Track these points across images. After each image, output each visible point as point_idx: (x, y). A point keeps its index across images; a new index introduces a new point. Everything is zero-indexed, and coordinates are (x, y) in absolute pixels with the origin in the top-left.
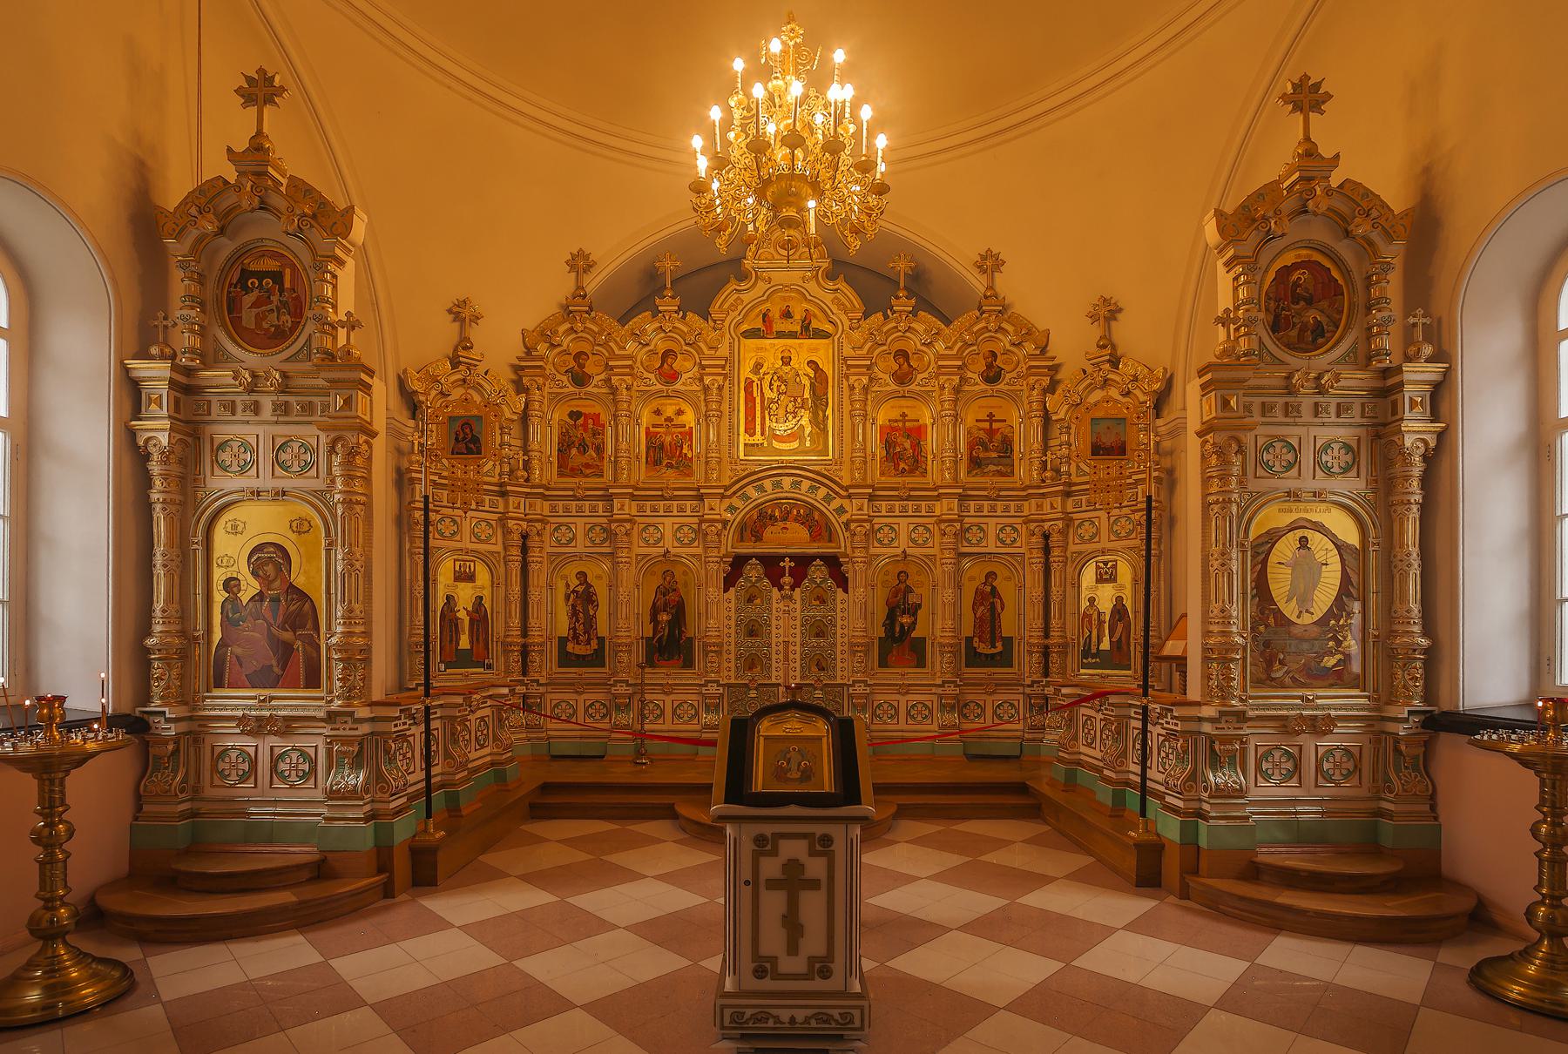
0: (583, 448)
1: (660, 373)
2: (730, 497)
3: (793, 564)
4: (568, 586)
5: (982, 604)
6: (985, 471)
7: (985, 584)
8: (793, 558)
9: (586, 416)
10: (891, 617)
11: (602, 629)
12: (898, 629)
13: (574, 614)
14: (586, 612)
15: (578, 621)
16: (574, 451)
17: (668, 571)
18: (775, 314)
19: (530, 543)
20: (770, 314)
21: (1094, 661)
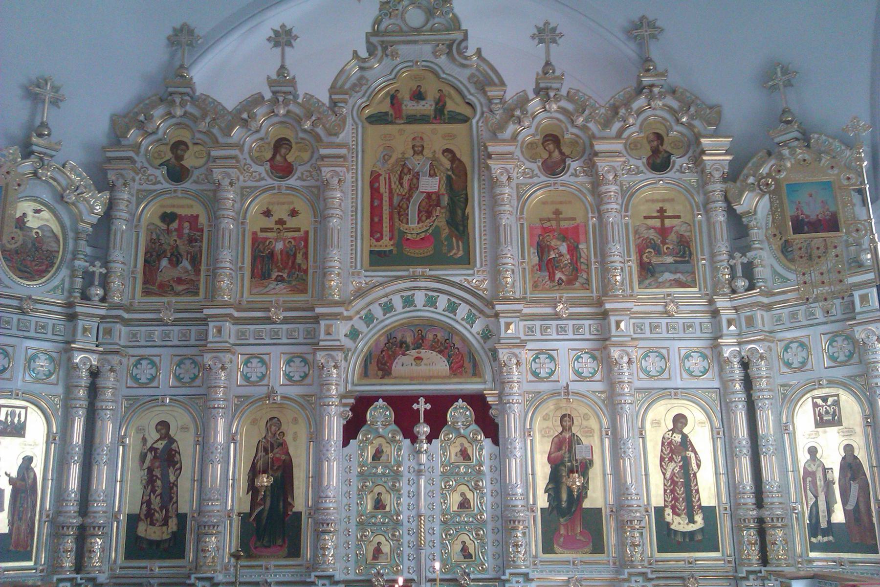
0: (175, 260)
1: (271, 166)
2: (350, 318)
3: (429, 406)
4: (144, 440)
5: (671, 459)
6: (660, 280)
7: (673, 430)
8: (429, 399)
9: (181, 218)
10: (555, 479)
11: (185, 502)
12: (564, 496)
13: (151, 480)
14: (165, 476)
15: (153, 491)
16: (164, 262)
17: (271, 419)
18: (405, 95)
19: (101, 382)
20: (399, 96)
21: (826, 539)
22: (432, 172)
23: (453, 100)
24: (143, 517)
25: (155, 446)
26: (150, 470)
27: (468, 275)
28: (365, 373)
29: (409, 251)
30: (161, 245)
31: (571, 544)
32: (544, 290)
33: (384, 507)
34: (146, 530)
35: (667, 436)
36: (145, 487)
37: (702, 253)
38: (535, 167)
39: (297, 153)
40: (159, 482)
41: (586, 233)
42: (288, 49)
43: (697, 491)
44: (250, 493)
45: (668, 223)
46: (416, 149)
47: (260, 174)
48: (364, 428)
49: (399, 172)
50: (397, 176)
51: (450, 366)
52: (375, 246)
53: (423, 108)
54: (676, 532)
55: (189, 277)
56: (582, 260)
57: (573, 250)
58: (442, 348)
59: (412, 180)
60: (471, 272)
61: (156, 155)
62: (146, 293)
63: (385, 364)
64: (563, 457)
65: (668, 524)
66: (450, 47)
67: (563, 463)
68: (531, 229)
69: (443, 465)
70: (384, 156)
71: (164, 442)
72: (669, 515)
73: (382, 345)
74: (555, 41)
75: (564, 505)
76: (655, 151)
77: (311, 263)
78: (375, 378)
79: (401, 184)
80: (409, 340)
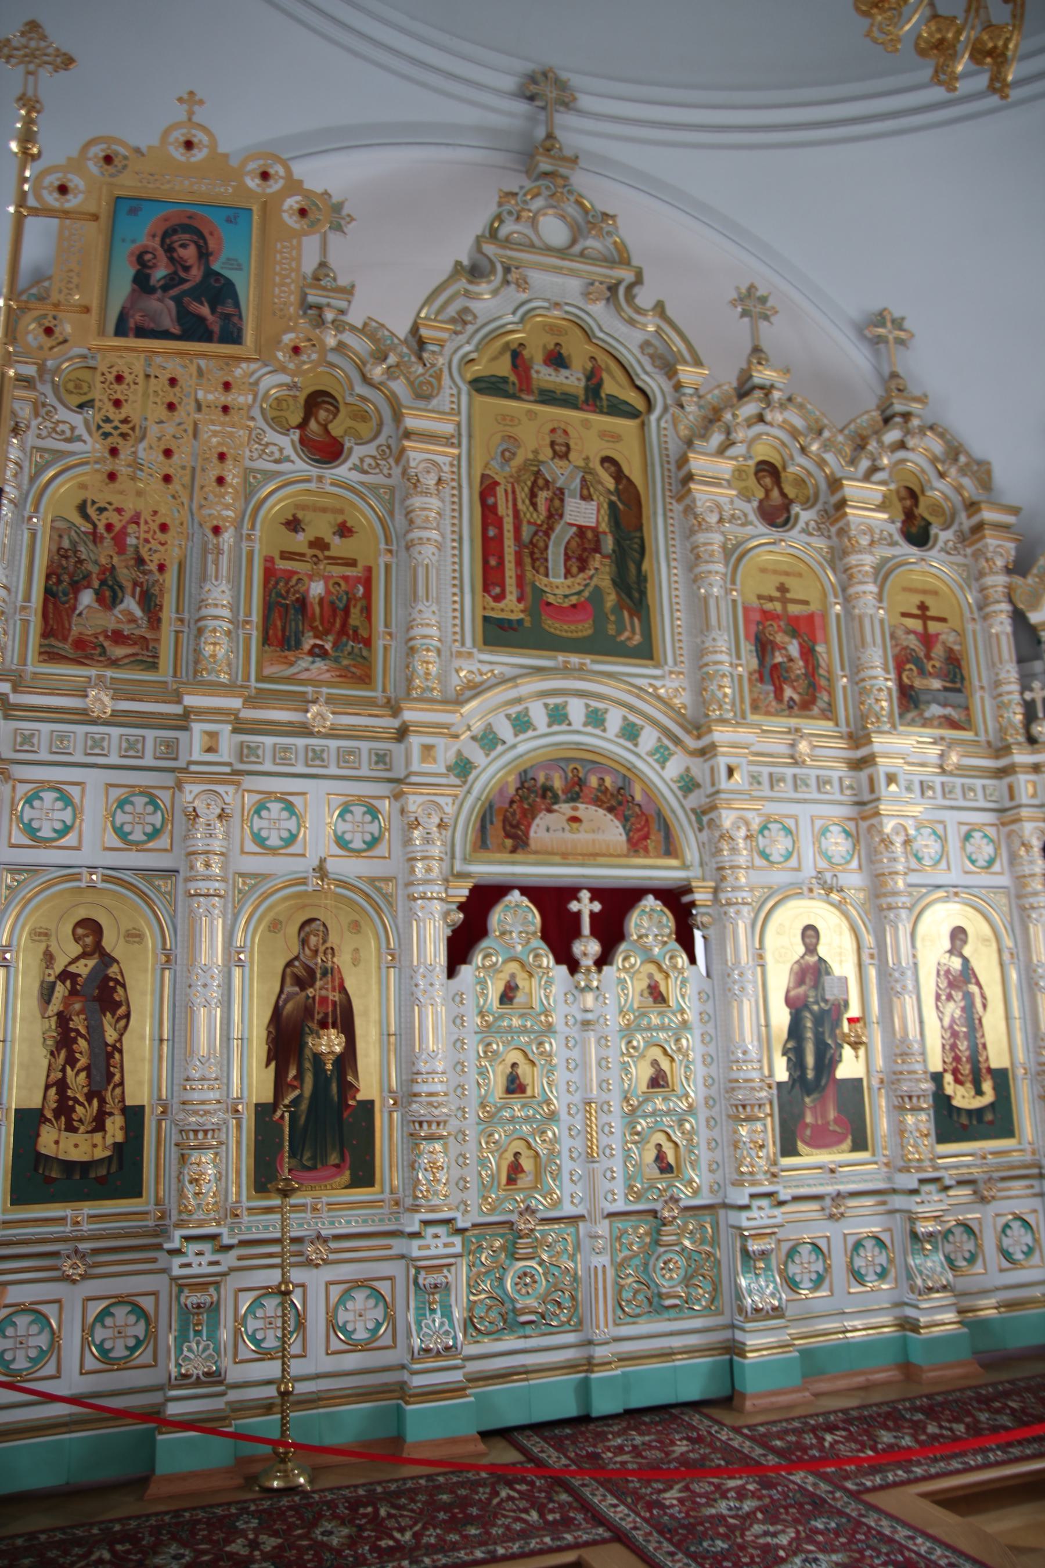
1: (302, 441)
3: (597, 907)
5: (950, 997)
6: (927, 714)
8: (597, 894)
14: (95, 1033)
15: (71, 1061)
16: (87, 598)
18: (535, 354)
22: (585, 492)
23: (613, 377)
24: (49, 1115)
25: (72, 969)
26: (63, 1019)
27: (655, 677)
28: (482, 842)
29: (553, 626)
30: (80, 561)
31: (821, 1140)
32: (768, 713)
33: (521, 1089)
34: (57, 1142)
35: (943, 961)
36: (52, 1053)
37: (980, 680)
38: (750, 509)
39: (350, 423)
40: (82, 1044)
41: (825, 627)
42: (333, 238)
43: (984, 1046)
44: (273, 1065)
45: (933, 627)
46: (557, 448)
47: (281, 450)
48: (485, 944)
49: (529, 483)
50: (526, 490)
51: (627, 834)
52: (493, 609)
53: (565, 381)
54: (959, 1109)
55: (137, 632)
56: (821, 672)
57: (808, 653)
58: (614, 803)
59: (551, 500)
60: (657, 672)
61: (71, 386)
62: (50, 655)
63: (516, 826)
64: (806, 996)
65: (949, 1098)
66: (613, 289)
67: (806, 1006)
68: (746, 610)
69: (622, 1012)
70: (503, 453)
71: (91, 963)
72: (950, 1087)
73: (511, 791)
74: (766, 318)
75: (810, 1075)
76: (909, 516)
77: (381, 628)
78: (499, 851)
79: (534, 505)
80: (558, 784)
